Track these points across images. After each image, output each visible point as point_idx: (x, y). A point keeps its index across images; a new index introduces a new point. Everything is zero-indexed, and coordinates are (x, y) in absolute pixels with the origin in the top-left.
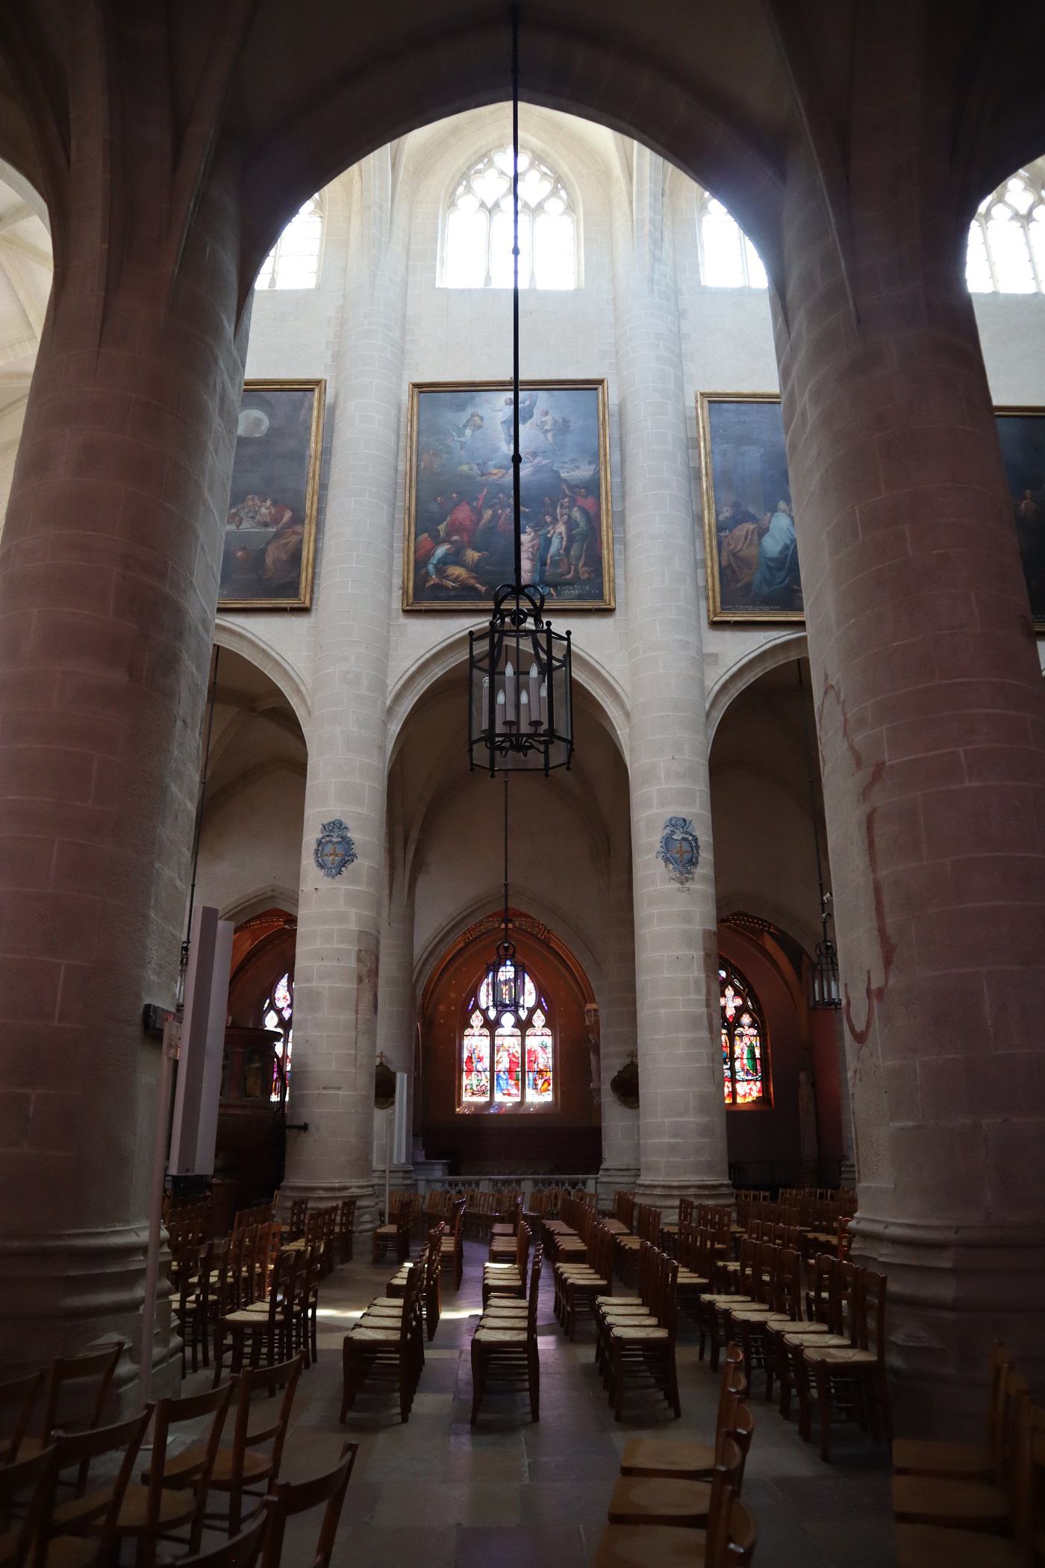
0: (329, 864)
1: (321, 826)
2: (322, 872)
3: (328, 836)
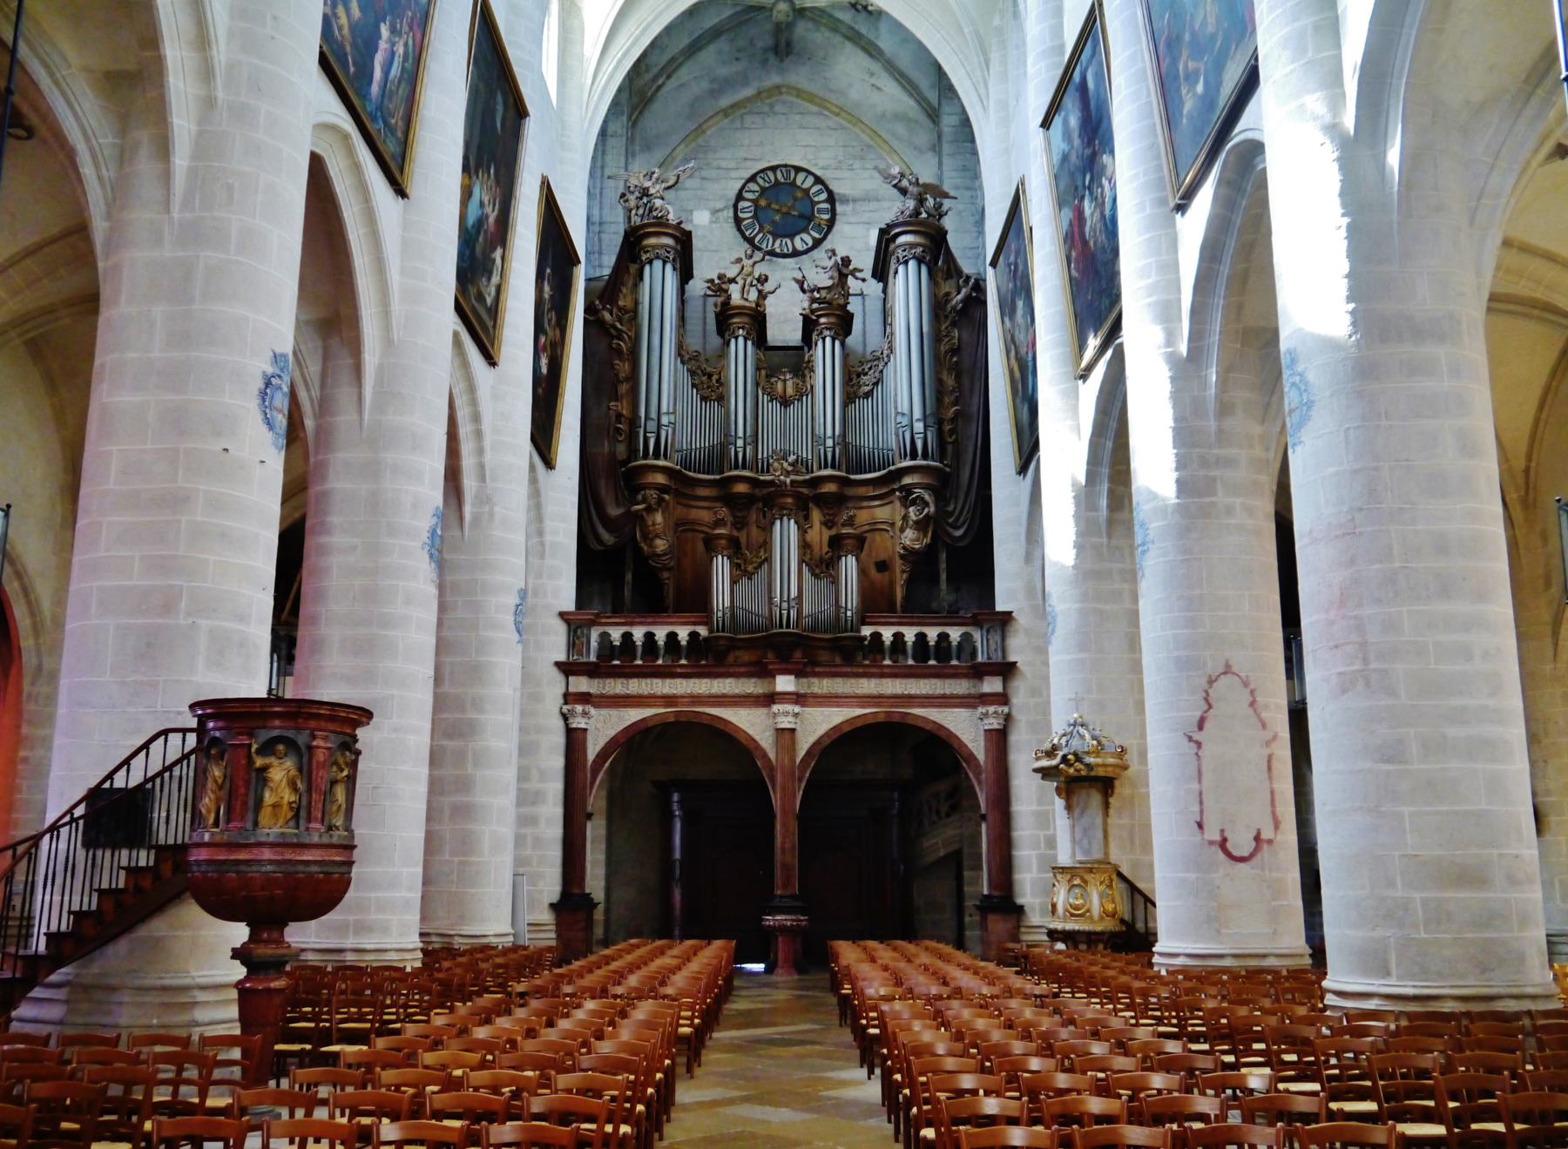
0: (277, 425)
1: (271, 354)
2: (268, 436)
3: (279, 376)
